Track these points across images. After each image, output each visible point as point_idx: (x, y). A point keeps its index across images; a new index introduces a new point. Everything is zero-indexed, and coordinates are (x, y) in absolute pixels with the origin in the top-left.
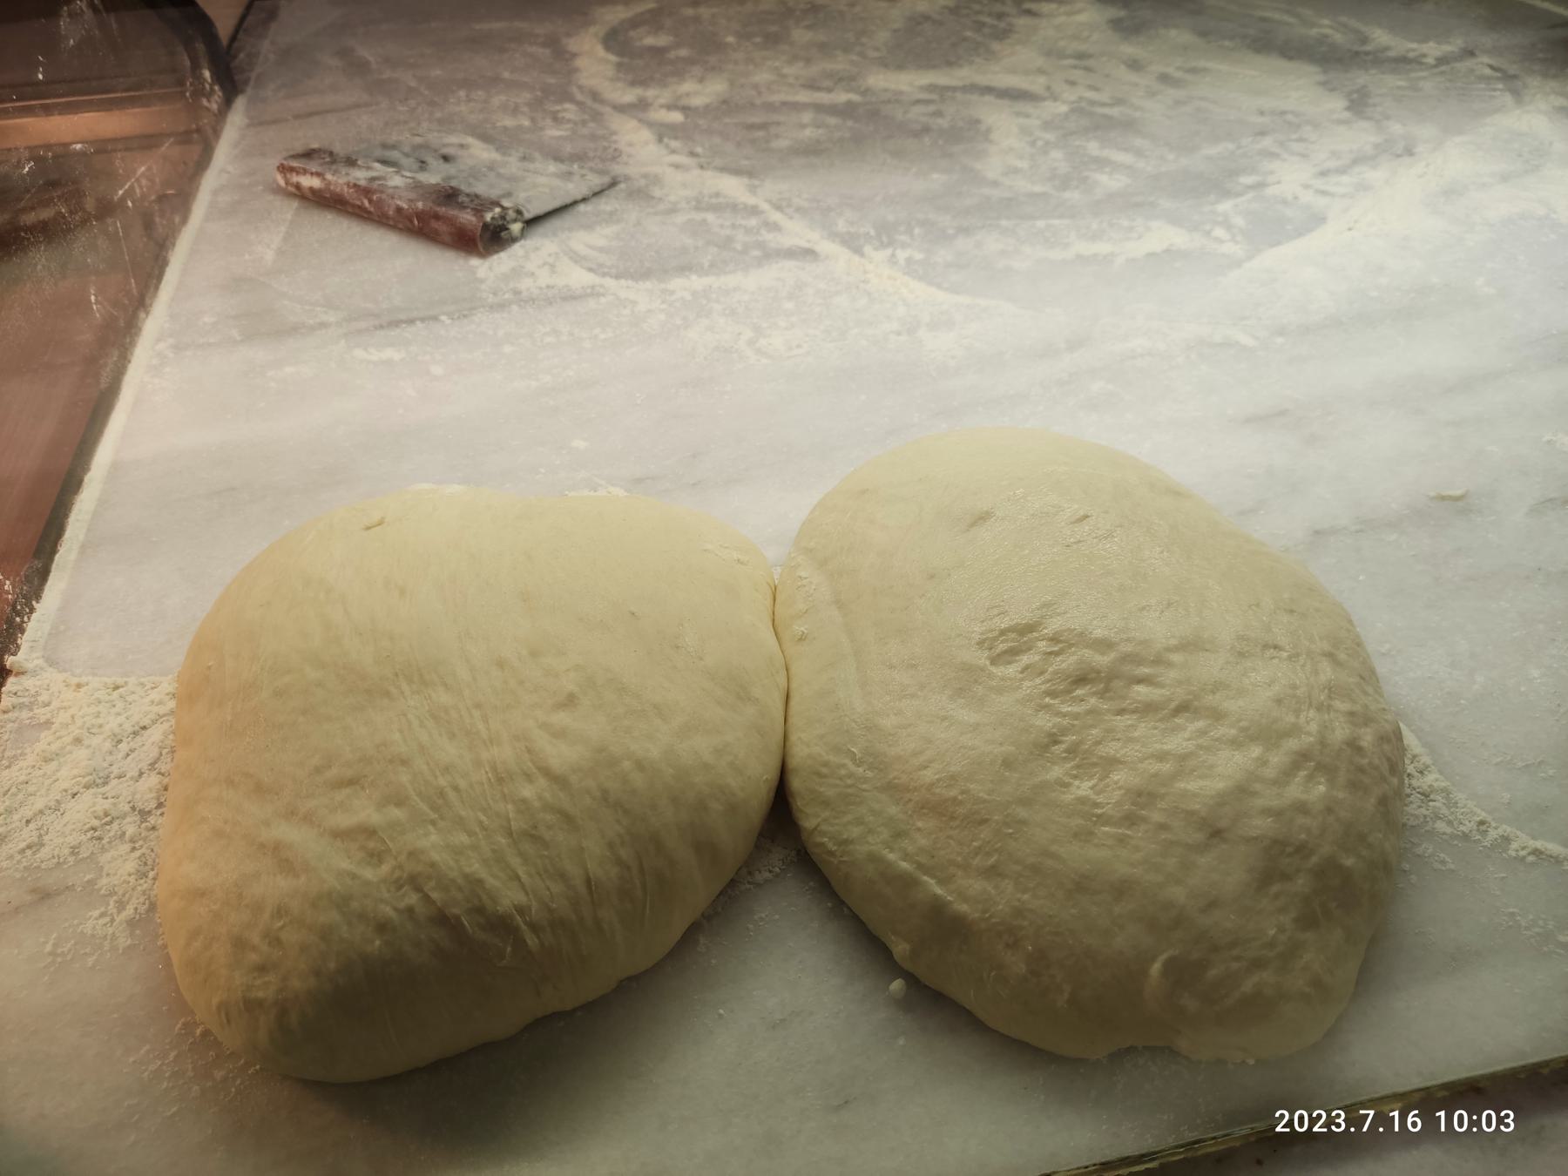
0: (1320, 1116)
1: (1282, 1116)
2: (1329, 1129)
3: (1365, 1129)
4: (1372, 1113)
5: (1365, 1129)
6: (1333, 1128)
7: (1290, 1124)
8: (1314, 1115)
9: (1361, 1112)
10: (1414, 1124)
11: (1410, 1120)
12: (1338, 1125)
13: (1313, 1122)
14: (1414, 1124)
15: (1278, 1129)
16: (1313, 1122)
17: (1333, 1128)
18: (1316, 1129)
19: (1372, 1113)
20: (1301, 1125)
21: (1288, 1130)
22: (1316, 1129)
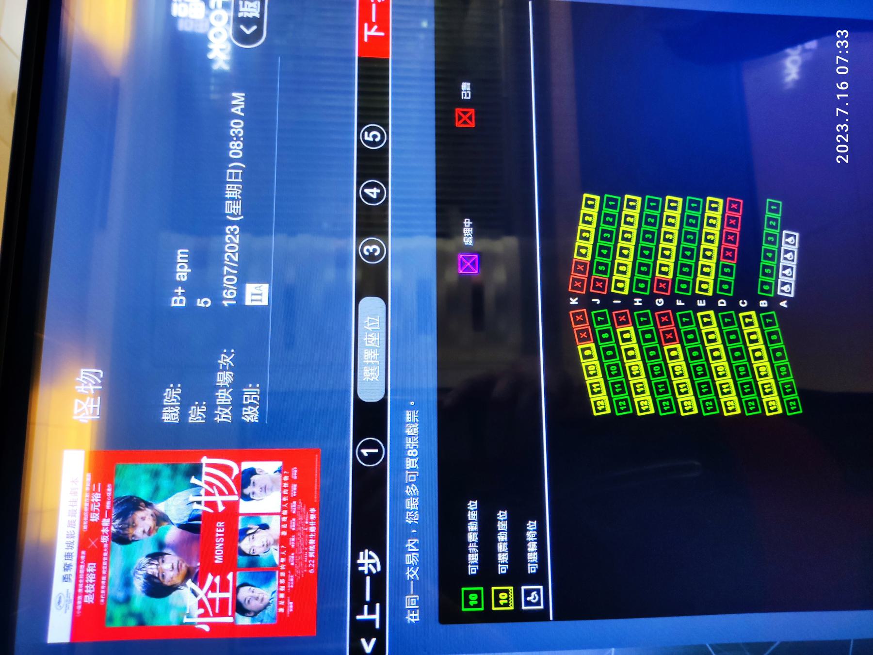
0: (840, 138)
1: (840, 159)
2: (847, 133)
3: (847, 113)
4: (838, 109)
5: (847, 113)
6: (846, 131)
7: (844, 155)
8: (839, 141)
9: (837, 115)
10: (844, 86)
11: (842, 88)
12: (845, 128)
13: (843, 142)
14: (844, 86)
15: (847, 161)
16: (843, 142)
17: (846, 131)
18: (847, 141)
19: (838, 109)
20: (845, 149)
21: (847, 156)
22: (847, 141)
